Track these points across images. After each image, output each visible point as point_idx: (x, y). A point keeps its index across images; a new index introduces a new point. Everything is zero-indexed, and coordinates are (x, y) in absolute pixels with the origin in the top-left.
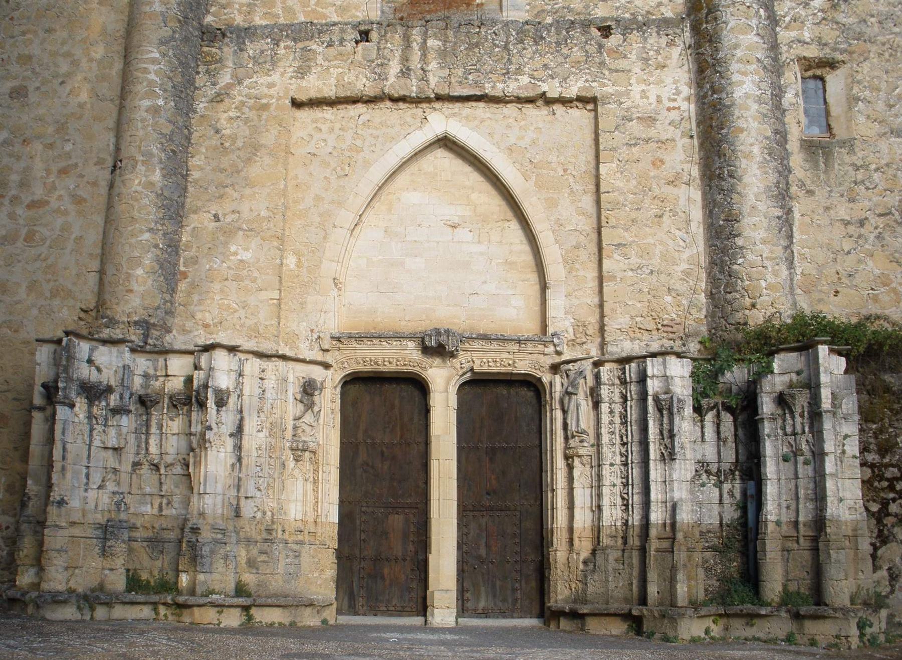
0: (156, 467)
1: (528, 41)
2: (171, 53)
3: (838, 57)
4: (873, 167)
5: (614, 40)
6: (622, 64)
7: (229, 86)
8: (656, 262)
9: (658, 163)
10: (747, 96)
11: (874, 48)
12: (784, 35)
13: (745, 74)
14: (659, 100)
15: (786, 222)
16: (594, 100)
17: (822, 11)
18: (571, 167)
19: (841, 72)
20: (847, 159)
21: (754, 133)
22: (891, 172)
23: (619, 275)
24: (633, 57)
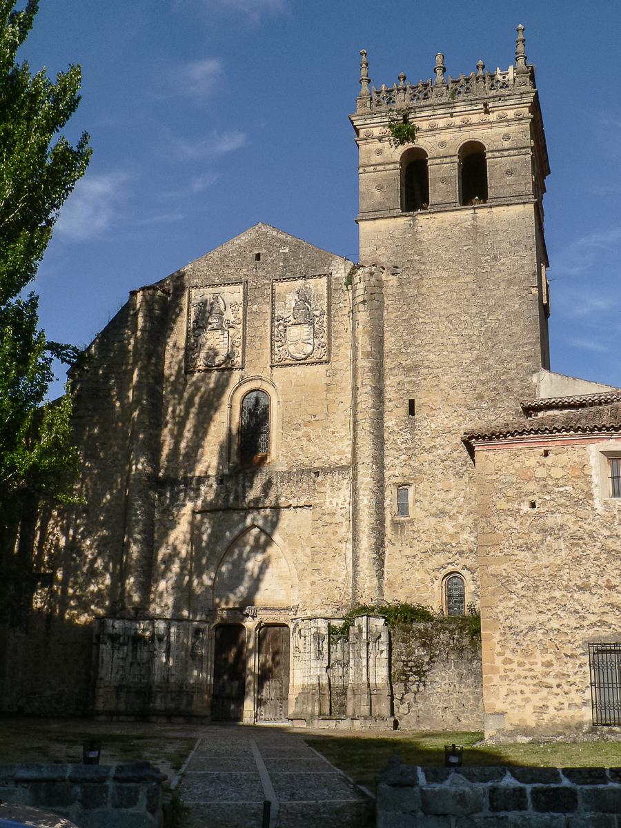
0: (139, 664)
1: (285, 481)
2: (143, 496)
3: (410, 481)
4: (421, 531)
5: (320, 478)
6: (323, 489)
7: (168, 505)
8: (332, 577)
9: (335, 533)
10: (365, 505)
11: (425, 477)
12: (387, 473)
13: (364, 495)
14: (337, 505)
15: (380, 561)
16: (310, 506)
17: (405, 461)
18: (302, 536)
19: (414, 486)
20: (410, 528)
21: (366, 522)
22: (429, 533)
23: (317, 582)
24: (327, 486)
